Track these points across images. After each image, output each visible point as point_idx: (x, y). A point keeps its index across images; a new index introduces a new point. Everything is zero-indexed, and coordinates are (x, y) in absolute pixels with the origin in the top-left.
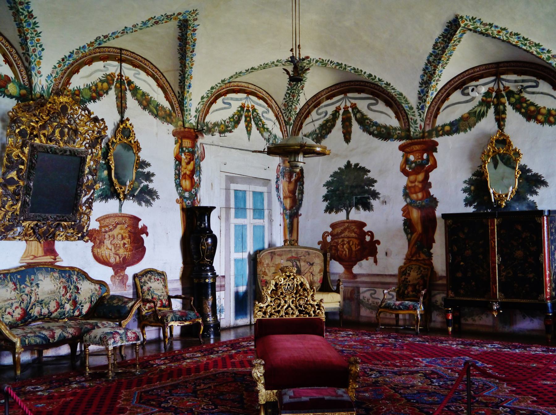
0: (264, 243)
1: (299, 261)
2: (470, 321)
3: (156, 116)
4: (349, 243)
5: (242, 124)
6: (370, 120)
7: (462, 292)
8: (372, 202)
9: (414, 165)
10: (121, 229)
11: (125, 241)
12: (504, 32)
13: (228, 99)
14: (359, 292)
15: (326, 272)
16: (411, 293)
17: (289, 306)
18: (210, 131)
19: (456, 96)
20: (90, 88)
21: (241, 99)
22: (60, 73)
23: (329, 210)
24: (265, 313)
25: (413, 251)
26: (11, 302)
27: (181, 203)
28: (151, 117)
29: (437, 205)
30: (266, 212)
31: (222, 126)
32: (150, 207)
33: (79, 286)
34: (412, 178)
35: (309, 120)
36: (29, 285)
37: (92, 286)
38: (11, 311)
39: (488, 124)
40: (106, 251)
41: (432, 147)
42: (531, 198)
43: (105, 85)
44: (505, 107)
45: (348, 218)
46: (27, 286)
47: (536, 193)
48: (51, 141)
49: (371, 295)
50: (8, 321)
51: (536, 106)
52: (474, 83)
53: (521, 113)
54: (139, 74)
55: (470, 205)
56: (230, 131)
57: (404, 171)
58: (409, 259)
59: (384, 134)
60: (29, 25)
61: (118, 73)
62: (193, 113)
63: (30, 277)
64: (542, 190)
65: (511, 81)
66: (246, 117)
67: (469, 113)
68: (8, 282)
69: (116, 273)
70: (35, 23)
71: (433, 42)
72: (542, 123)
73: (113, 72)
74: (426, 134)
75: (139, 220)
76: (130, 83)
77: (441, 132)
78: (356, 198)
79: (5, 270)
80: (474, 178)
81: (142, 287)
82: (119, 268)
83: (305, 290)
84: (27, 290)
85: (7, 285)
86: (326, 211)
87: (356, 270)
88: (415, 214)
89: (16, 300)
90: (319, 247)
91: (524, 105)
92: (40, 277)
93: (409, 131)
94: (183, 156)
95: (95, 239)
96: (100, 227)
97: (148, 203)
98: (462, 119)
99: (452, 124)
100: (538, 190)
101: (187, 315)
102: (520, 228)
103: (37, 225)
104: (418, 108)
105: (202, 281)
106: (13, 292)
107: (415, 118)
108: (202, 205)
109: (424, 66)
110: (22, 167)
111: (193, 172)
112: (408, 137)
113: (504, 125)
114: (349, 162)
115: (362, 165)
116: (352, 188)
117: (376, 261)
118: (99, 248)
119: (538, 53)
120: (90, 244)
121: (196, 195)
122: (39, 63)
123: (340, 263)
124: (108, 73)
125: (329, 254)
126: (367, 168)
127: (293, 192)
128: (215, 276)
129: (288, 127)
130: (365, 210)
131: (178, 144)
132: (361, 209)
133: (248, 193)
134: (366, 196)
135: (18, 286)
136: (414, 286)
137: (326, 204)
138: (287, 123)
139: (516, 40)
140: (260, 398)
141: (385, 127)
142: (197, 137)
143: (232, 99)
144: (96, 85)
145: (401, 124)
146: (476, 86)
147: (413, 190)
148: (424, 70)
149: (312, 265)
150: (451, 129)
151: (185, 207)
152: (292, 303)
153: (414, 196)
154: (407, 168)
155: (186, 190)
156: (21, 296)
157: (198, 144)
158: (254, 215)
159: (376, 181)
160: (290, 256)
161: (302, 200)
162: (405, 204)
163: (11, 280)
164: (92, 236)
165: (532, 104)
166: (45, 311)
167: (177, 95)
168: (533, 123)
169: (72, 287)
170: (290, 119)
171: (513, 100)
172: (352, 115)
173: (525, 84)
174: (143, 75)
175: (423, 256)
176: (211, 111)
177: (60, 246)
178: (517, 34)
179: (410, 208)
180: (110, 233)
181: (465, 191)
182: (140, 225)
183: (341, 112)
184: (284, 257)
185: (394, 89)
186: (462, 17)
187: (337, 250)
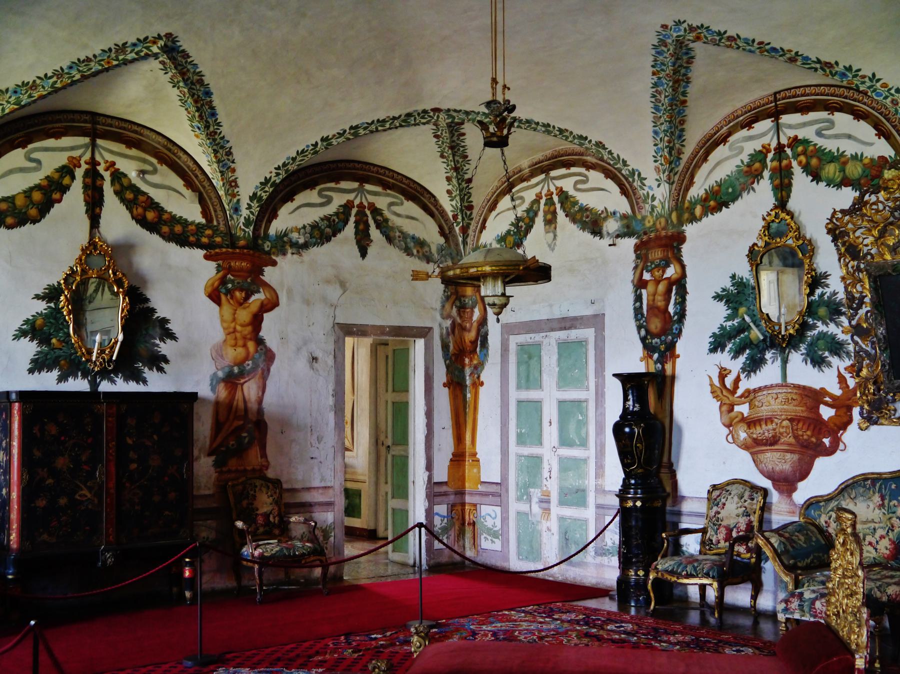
26: (872, 525)
38: (874, 542)
50: (872, 556)
60: (843, 75)
68: (874, 493)
79: (873, 474)
85: (870, 498)
89: (881, 525)
106: (877, 511)
135: (886, 502)
156: (890, 518)
163: (880, 488)
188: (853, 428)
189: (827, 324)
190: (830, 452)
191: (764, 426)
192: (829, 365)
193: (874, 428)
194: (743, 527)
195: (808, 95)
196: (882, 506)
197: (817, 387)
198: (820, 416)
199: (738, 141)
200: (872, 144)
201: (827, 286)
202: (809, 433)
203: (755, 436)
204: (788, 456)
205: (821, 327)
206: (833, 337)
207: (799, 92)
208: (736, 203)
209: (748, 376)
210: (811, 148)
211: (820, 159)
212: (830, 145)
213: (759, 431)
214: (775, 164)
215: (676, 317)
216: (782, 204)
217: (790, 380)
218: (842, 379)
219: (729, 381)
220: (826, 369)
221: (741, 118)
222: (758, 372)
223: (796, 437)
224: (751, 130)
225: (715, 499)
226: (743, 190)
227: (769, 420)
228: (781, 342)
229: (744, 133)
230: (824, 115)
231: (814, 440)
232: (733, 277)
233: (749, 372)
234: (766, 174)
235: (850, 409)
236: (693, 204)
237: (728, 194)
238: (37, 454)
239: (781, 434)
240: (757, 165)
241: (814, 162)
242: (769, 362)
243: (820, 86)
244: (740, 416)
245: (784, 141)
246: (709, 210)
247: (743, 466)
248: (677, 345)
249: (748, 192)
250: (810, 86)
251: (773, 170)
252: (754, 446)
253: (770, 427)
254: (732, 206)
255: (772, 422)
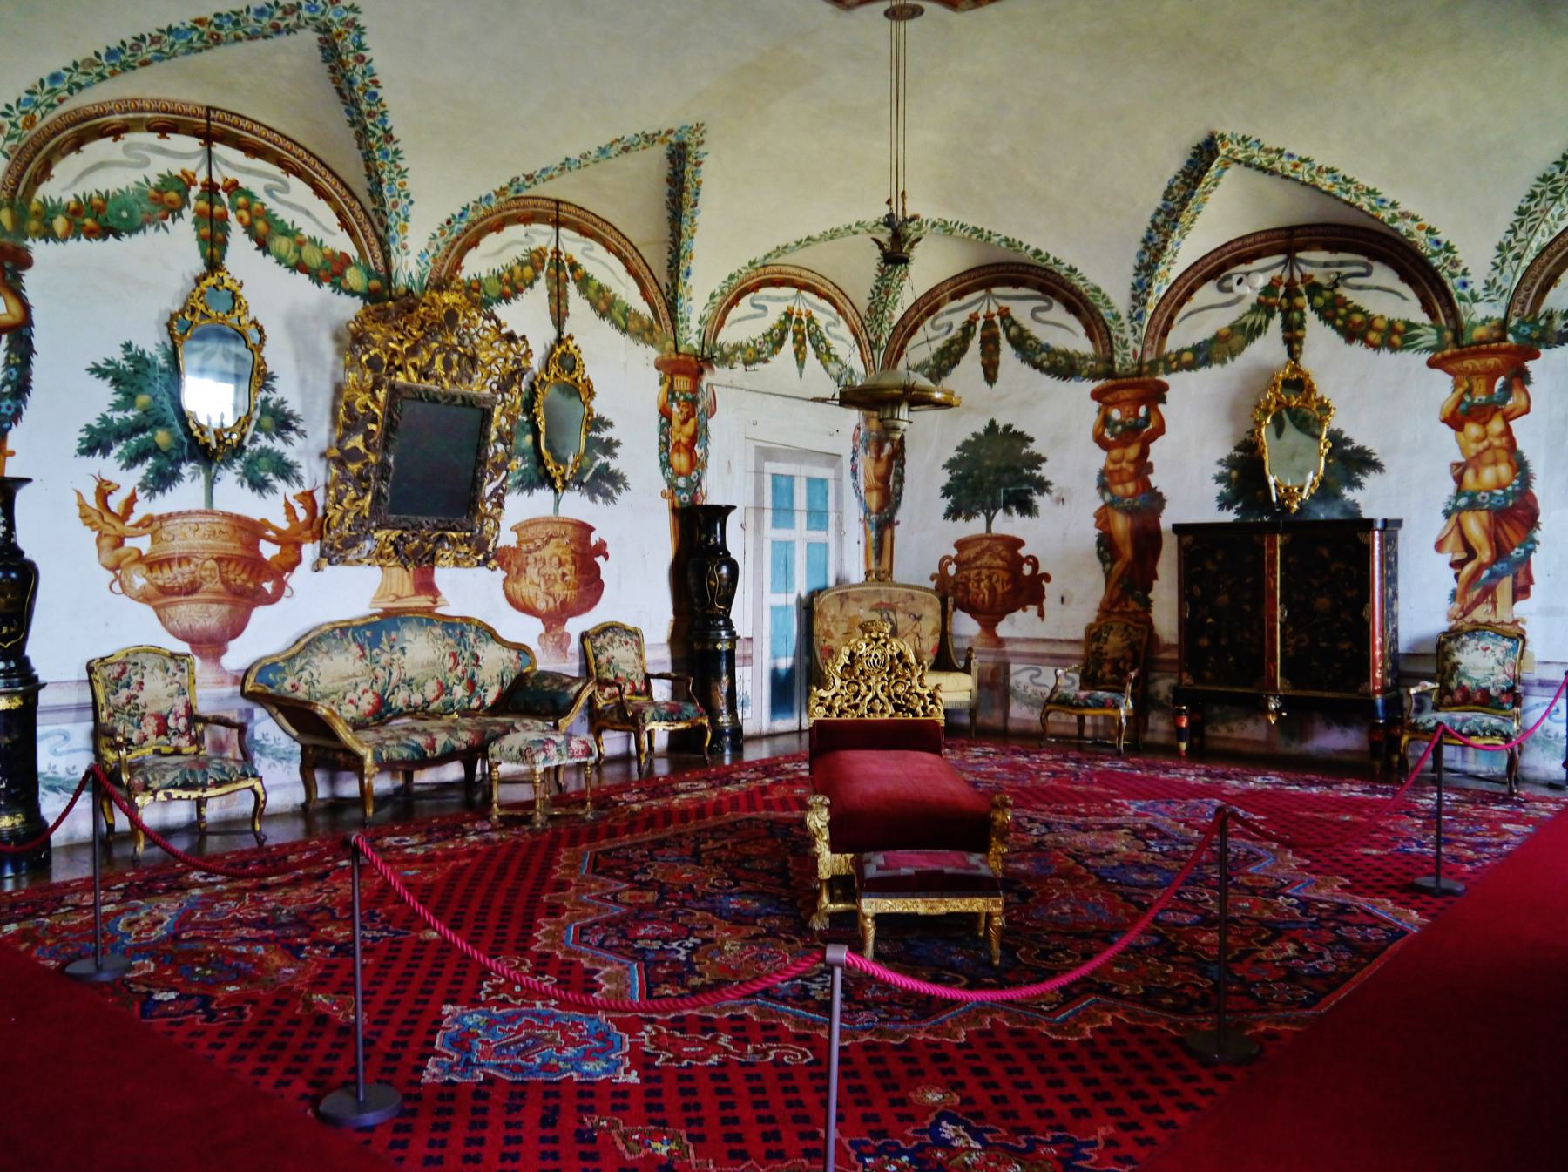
0: (826, 575)
1: (895, 612)
2: (1222, 731)
3: (624, 331)
4: (990, 577)
5: (789, 346)
6: (1035, 339)
7: (1208, 674)
8: (1037, 499)
9: (1119, 428)
10: (558, 546)
11: (566, 569)
12: (1306, 166)
13: (761, 298)
14: (1007, 673)
15: (944, 634)
16: (1108, 676)
17: (876, 696)
18: (726, 360)
19: (1207, 293)
20: (499, 277)
21: (786, 299)
22: (443, 247)
23: (953, 513)
24: (830, 709)
25: (1116, 595)
26: (354, 680)
27: (672, 498)
28: (616, 333)
29: (1162, 507)
30: (832, 517)
31: (750, 351)
32: (611, 506)
33: (480, 654)
34: (1116, 453)
35: (914, 340)
36: (387, 649)
37: (506, 654)
38: (355, 697)
39: (1268, 349)
40: (529, 588)
41: (1157, 394)
42: (1349, 494)
43: (528, 270)
44: (1302, 315)
45: (989, 529)
46: (383, 651)
47: (1360, 485)
48: (427, 378)
49: (1031, 678)
51: (1365, 313)
52: (1242, 268)
53: (1334, 327)
54: (592, 249)
55: (1229, 508)
56: (765, 361)
57: (1100, 440)
58: (1106, 610)
59: (1063, 367)
60: (386, 155)
61: (552, 246)
62: (694, 325)
63: (389, 634)
64: (1371, 480)
65: (1316, 263)
66: (795, 333)
67: (1232, 327)
69: (548, 629)
70: (396, 152)
71: (1164, 186)
72: (1376, 347)
73: (543, 245)
74: (1145, 368)
75: (592, 529)
76: (574, 266)
77: (1174, 365)
78: (1006, 492)
80: (1238, 454)
81: (596, 657)
82: (554, 619)
83: (906, 666)
84: (384, 659)
86: (947, 516)
87: (1003, 629)
88: (1121, 524)
90: (932, 585)
91: (1342, 311)
92: (408, 634)
93: (1111, 361)
94: (675, 409)
95: (509, 564)
96: (519, 542)
97: (607, 496)
98: (1218, 338)
99: (1196, 349)
100: (1363, 480)
101: (680, 711)
102: (1325, 553)
103: (401, 537)
104: (1130, 317)
105: (710, 646)
106: (359, 663)
107: (1124, 337)
108: (710, 502)
109: (1144, 234)
110: (373, 427)
111: (693, 439)
112: (1110, 374)
113: (1300, 351)
114: (992, 422)
115: (1018, 427)
116: (998, 473)
117: (1041, 614)
118: (517, 581)
119: (1373, 208)
120: (500, 574)
121: (699, 483)
122: (404, 228)
123: (973, 616)
124: (533, 248)
125: (950, 600)
126: (1028, 433)
127: (884, 479)
128: (733, 638)
129: (876, 352)
130: (1022, 515)
131: (666, 386)
132: (1015, 512)
133: (797, 481)
134: (1025, 487)
135: (367, 651)
136: (1115, 662)
137: (947, 502)
138: (874, 345)
139: (1329, 182)
140: (821, 867)
141: (1066, 354)
142: (701, 372)
143: (768, 298)
144: (511, 272)
145: (1096, 348)
146: (1248, 274)
147: (1116, 477)
148: (1144, 242)
149: (918, 618)
150: (1195, 358)
151: (678, 505)
152: (882, 690)
153: (1119, 489)
154: (1107, 435)
155: (680, 474)
157: (704, 385)
158: (809, 521)
159: (1044, 460)
160: (876, 601)
161: (900, 494)
162: (1100, 503)
163: (354, 639)
164: (502, 558)
165: (1358, 310)
166: (417, 699)
167: (665, 290)
168: (1357, 348)
169: (467, 655)
170: (879, 338)
171: (1319, 301)
172: (1001, 330)
173: (1345, 270)
174: (599, 250)
175: (1133, 606)
176: (727, 321)
177: (444, 576)
178: (1331, 171)
179: (1110, 511)
180: (538, 554)
181: (1220, 479)
182: (594, 539)
183: (980, 324)
184: (866, 603)
185: (1083, 279)
186: (1222, 137)
187: (967, 591)
188: (303, 569)
189: (272, 439)
190: (272, 599)
191: (175, 568)
192: (274, 490)
193: (328, 569)
194: (182, 711)
195: (255, 134)
196: (364, 656)
197: (257, 517)
198: (259, 554)
199: (140, 146)
200: (333, 234)
201: (273, 390)
202: (244, 576)
203: (160, 582)
204: (214, 608)
205: (264, 441)
206: (280, 457)
207: (256, 128)
208: (135, 237)
209: (151, 495)
210: (257, 206)
211: (269, 226)
212: (284, 214)
213: (165, 576)
214: (203, 205)
215: (8, 388)
216: (214, 264)
217: (219, 505)
218: (290, 510)
219: (115, 502)
220: (269, 496)
221: (149, 115)
222: (167, 491)
223: (225, 582)
224: (164, 141)
225: (119, 678)
226: (148, 221)
227: (184, 559)
228: (207, 452)
229: (152, 138)
230: (277, 171)
231: (251, 585)
232: (128, 346)
233: (153, 491)
234: (188, 213)
235: (298, 546)
236: (47, 214)
237: (120, 218)
238: (1197, 591)
239: (203, 578)
240: (172, 195)
241: (260, 225)
242: (187, 479)
243: (274, 131)
244: (135, 555)
245: (217, 179)
246: (76, 230)
247: (139, 627)
248: (10, 434)
249: (157, 229)
250: (260, 125)
251: (200, 214)
252: (160, 598)
253: (186, 568)
254: (125, 238)
255: (189, 562)
